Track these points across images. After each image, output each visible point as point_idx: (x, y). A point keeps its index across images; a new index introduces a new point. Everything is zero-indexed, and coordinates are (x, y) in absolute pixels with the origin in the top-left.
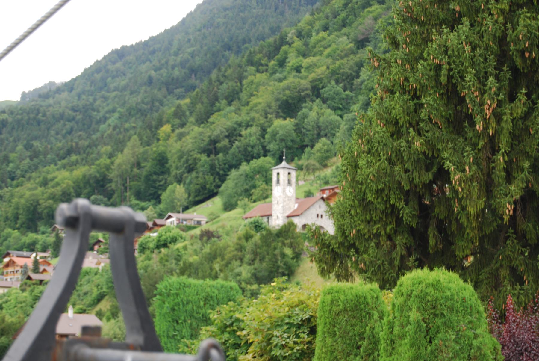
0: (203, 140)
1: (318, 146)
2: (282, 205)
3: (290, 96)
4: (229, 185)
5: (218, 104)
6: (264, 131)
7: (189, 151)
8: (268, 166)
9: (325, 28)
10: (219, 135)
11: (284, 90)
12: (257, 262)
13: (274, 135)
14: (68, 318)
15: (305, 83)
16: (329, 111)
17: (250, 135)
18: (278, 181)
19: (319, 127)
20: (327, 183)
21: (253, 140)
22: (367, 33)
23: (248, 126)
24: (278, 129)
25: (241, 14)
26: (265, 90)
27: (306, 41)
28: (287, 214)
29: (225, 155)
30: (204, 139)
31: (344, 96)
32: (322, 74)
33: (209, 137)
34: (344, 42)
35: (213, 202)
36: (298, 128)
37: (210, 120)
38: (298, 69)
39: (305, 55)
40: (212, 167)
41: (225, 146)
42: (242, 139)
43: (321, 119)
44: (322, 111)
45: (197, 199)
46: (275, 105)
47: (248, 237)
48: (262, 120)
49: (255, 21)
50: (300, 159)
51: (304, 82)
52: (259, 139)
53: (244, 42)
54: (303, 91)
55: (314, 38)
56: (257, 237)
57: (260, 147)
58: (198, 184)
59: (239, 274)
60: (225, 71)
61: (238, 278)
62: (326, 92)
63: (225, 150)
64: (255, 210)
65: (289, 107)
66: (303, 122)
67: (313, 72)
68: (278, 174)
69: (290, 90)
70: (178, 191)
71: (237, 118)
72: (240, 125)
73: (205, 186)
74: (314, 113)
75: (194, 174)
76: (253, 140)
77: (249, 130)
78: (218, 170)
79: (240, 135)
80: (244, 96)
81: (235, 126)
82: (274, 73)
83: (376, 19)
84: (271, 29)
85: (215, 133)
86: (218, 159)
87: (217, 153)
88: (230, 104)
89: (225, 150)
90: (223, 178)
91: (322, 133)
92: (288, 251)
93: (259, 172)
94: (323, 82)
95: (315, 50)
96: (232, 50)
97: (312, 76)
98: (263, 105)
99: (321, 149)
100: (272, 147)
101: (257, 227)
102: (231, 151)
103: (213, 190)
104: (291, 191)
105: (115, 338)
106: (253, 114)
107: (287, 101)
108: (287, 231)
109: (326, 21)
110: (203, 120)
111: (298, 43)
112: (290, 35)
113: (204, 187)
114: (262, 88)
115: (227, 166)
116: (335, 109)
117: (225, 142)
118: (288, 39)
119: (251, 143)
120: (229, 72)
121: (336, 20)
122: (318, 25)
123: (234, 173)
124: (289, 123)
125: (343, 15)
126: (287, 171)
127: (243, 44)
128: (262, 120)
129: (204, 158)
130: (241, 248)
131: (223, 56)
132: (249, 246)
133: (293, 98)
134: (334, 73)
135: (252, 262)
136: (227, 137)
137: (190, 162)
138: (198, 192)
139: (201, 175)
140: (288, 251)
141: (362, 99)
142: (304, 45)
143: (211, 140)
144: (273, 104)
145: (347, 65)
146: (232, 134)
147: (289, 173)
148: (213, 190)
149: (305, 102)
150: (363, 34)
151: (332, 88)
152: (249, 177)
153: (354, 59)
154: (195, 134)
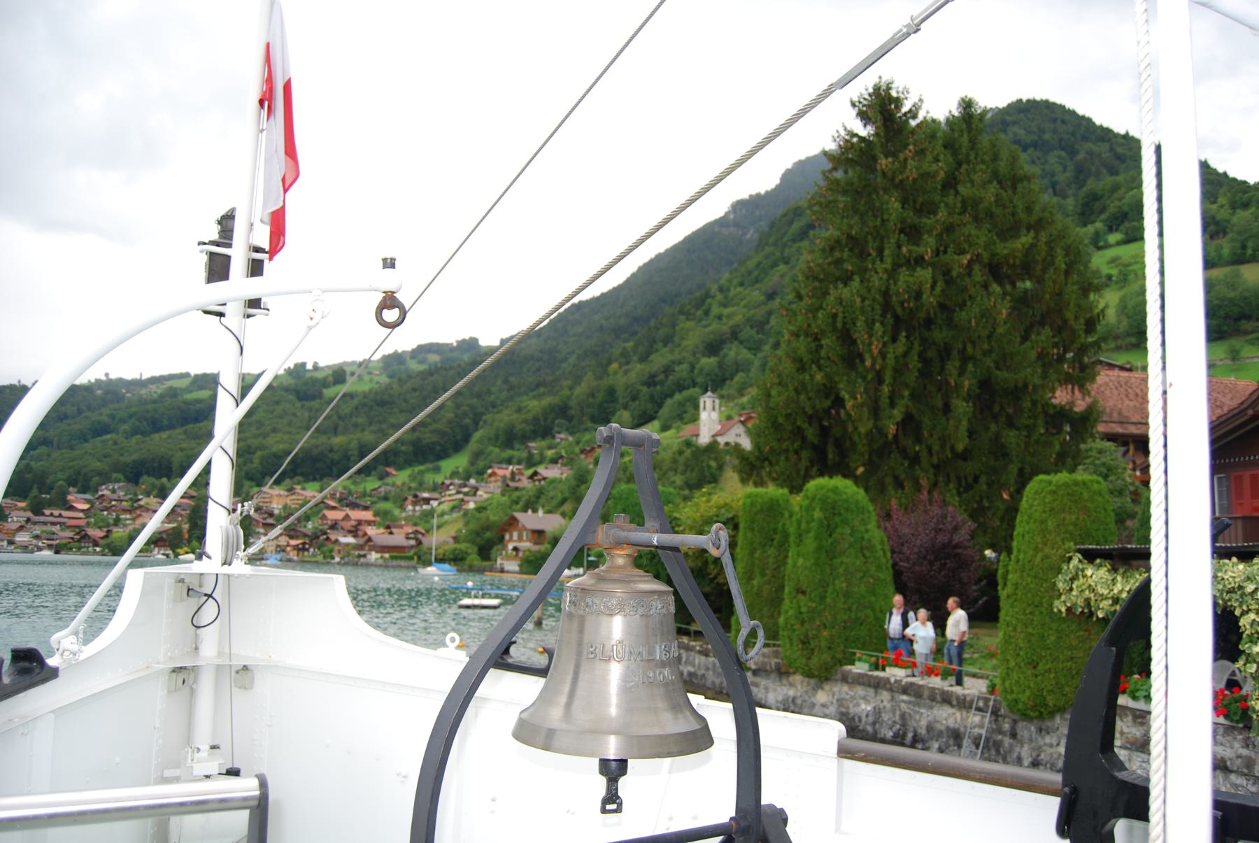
1: (737, 379)
4: (665, 411)
6: (693, 367)
9: (742, 284)
12: (688, 474)
13: (701, 370)
15: (726, 329)
16: (745, 351)
17: (682, 370)
19: (737, 364)
20: (744, 408)
23: (680, 363)
26: (693, 334)
34: (756, 295)
36: (720, 365)
37: (651, 358)
38: (720, 317)
39: (725, 306)
40: (652, 397)
47: (680, 453)
48: (691, 359)
53: (676, 296)
55: (733, 292)
56: (688, 452)
62: (742, 335)
63: (662, 383)
64: (687, 430)
65: (713, 348)
71: (670, 357)
72: (673, 362)
74: (733, 352)
75: (637, 402)
76: (684, 374)
77: (681, 367)
80: (676, 339)
82: (701, 320)
83: (782, 276)
87: (655, 385)
88: (665, 345)
89: (662, 383)
90: (660, 406)
92: (713, 464)
97: (731, 323)
100: (700, 380)
101: (688, 444)
104: (715, 415)
106: (684, 354)
108: (712, 447)
110: (644, 358)
111: (719, 297)
113: (645, 413)
116: (750, 349)
117: (661, 377)
122: (735, 282)
123: (669, 402)
125: (756, 273)
128: (691, 359)
129: (645, 389)
130: (675, 461)
132: (682, 459)
134: (748, 320)
135: (684, 473)
140: (713, 464)
141: (772, 340)
145: (759, 313)
146: (667, 370)
151: (747, 332)
152: (681, 404)
153: (764, 309)
154: (638, 370)
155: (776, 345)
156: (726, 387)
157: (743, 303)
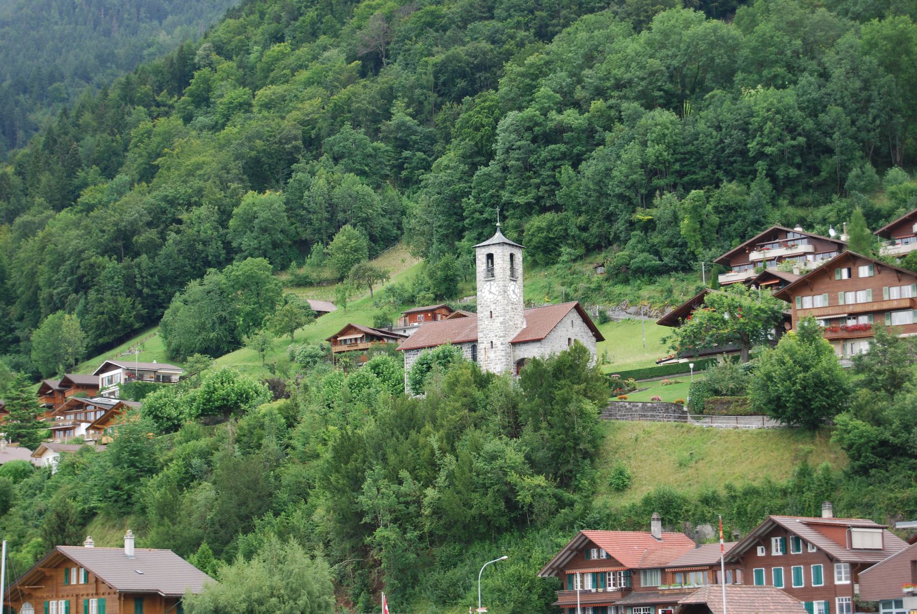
0: (103, 231)
1: (339, 239)
2: (501, 319)
3: (264, 151)
4: (181, 311)
5: (81, 174)
6: (225, 215)
7: (78, 253)
8: (263, 274)
10: (135, 220)
11: (249, 139)
13: (249, 219)
14: (126, 556)
17: (200, 220)
18: (490, 272)
19: (332, 208)
20: (411, 301)
21: (207, 229)
22: (373, 44)
23: (189, 205)
24: (255, 209)
25: (33, 33)
27: (241, 61)
28: (510, 340)
29: (152, 258)
30: (105, 228)
31: (369, 150)
32: (313, 112)
33: (116, 224)
35: (142, 344)
36: (292, 207)
40: (129, 281)
41: (151, 241)
42: (182, 227)
43: (337, 191)
44: (335, 177)
45: (101, 341)
46: (236, 168)
49: (60, 45)
50: (300, 266)
51: (289, 124)
52: (216, 229)
53: (52, 79)
54: (289, 141)
57: (220, 242)
58: (102, 313)
59: (493, 457)
60: (78, 117)
61: (500, 462)
63: (153, 248)
65: (262, 171)
66: (301, 198)
67: (295, 108)
68: (490, 257)
69: (260, 139)
70: (69, 326)
72: (172, 202)
73: (116, 317)
74: (320, 180)
75: (92, 295)
76: (207, 229)
77: (196, 211)
78: (138, 286)
79: (180, 222)
81: (163, 204)
84: (98, 57)
85: (127, 217)
86: (138, 266)
89: (153, 248)
91: (340, 216)
93: (245, 286)
94: (318, 125)
95: (272, 75)
96: (31, 92)
98: (214, 165)
99: (345, 245)
102: (163, 252)
103: (132, 325)
104: (516, 291)
105: (272, 595)
107: (257, 161)
109: (274, 25)
110: (65, 198)
112: (200, 52)
113: (114, 319)
114: (177, 142)
115: (156, 279)
116: (362, 173)
118: (196, 60)
119: (203, 235)
120: (87, 117)
121: (298, 24)
122: (258, 34)
124: (273, 197)
126: (508, 250)
127: (50, 84)
129: (110, 264)
131: (17, 103)
133: (270, 155)
136: (149, 224)
137: (81, 271)
138: (102, 329)
139: (107, 296)
142: (239, 67)
143: (119, 230)
144: (232, 165)
146: (163, 218)
147: (512, 256)
148: (132, 325)
149: (297, 161)
150: (366, 46)
155: (481, 153)
156: (312, 259)
157: (303, 75)
